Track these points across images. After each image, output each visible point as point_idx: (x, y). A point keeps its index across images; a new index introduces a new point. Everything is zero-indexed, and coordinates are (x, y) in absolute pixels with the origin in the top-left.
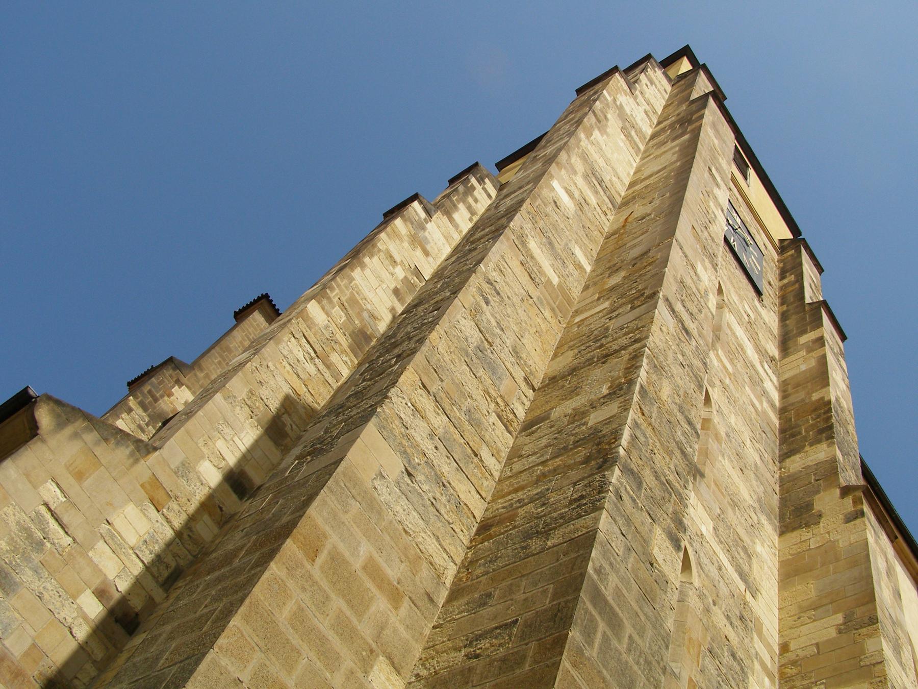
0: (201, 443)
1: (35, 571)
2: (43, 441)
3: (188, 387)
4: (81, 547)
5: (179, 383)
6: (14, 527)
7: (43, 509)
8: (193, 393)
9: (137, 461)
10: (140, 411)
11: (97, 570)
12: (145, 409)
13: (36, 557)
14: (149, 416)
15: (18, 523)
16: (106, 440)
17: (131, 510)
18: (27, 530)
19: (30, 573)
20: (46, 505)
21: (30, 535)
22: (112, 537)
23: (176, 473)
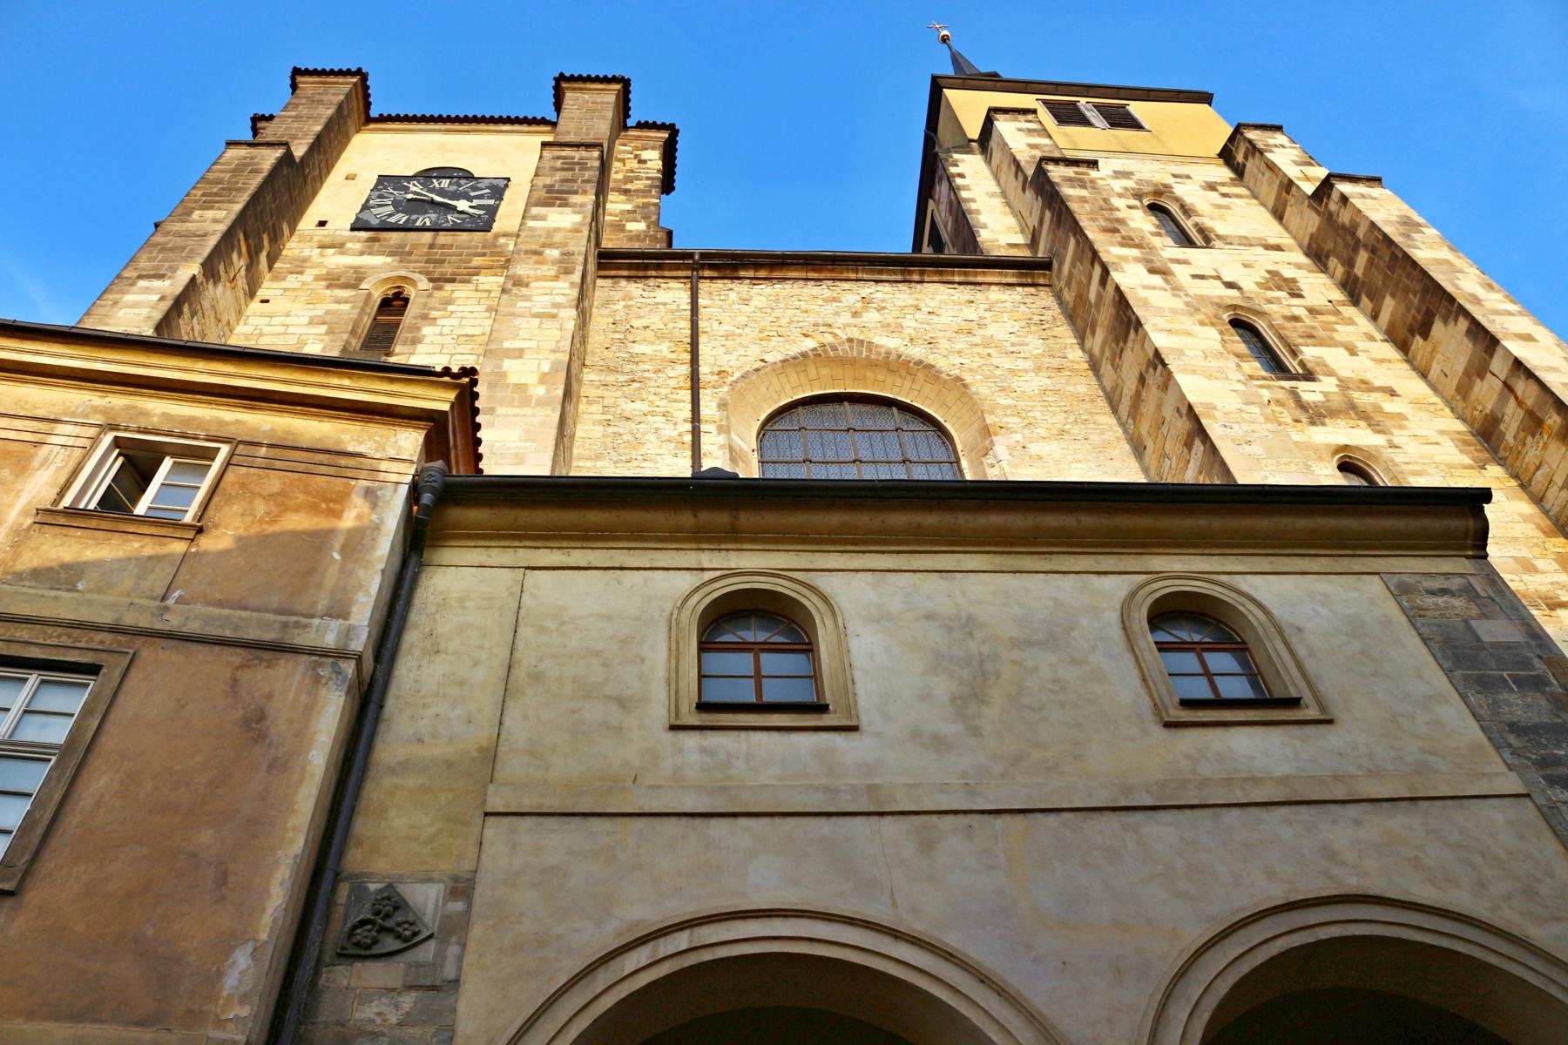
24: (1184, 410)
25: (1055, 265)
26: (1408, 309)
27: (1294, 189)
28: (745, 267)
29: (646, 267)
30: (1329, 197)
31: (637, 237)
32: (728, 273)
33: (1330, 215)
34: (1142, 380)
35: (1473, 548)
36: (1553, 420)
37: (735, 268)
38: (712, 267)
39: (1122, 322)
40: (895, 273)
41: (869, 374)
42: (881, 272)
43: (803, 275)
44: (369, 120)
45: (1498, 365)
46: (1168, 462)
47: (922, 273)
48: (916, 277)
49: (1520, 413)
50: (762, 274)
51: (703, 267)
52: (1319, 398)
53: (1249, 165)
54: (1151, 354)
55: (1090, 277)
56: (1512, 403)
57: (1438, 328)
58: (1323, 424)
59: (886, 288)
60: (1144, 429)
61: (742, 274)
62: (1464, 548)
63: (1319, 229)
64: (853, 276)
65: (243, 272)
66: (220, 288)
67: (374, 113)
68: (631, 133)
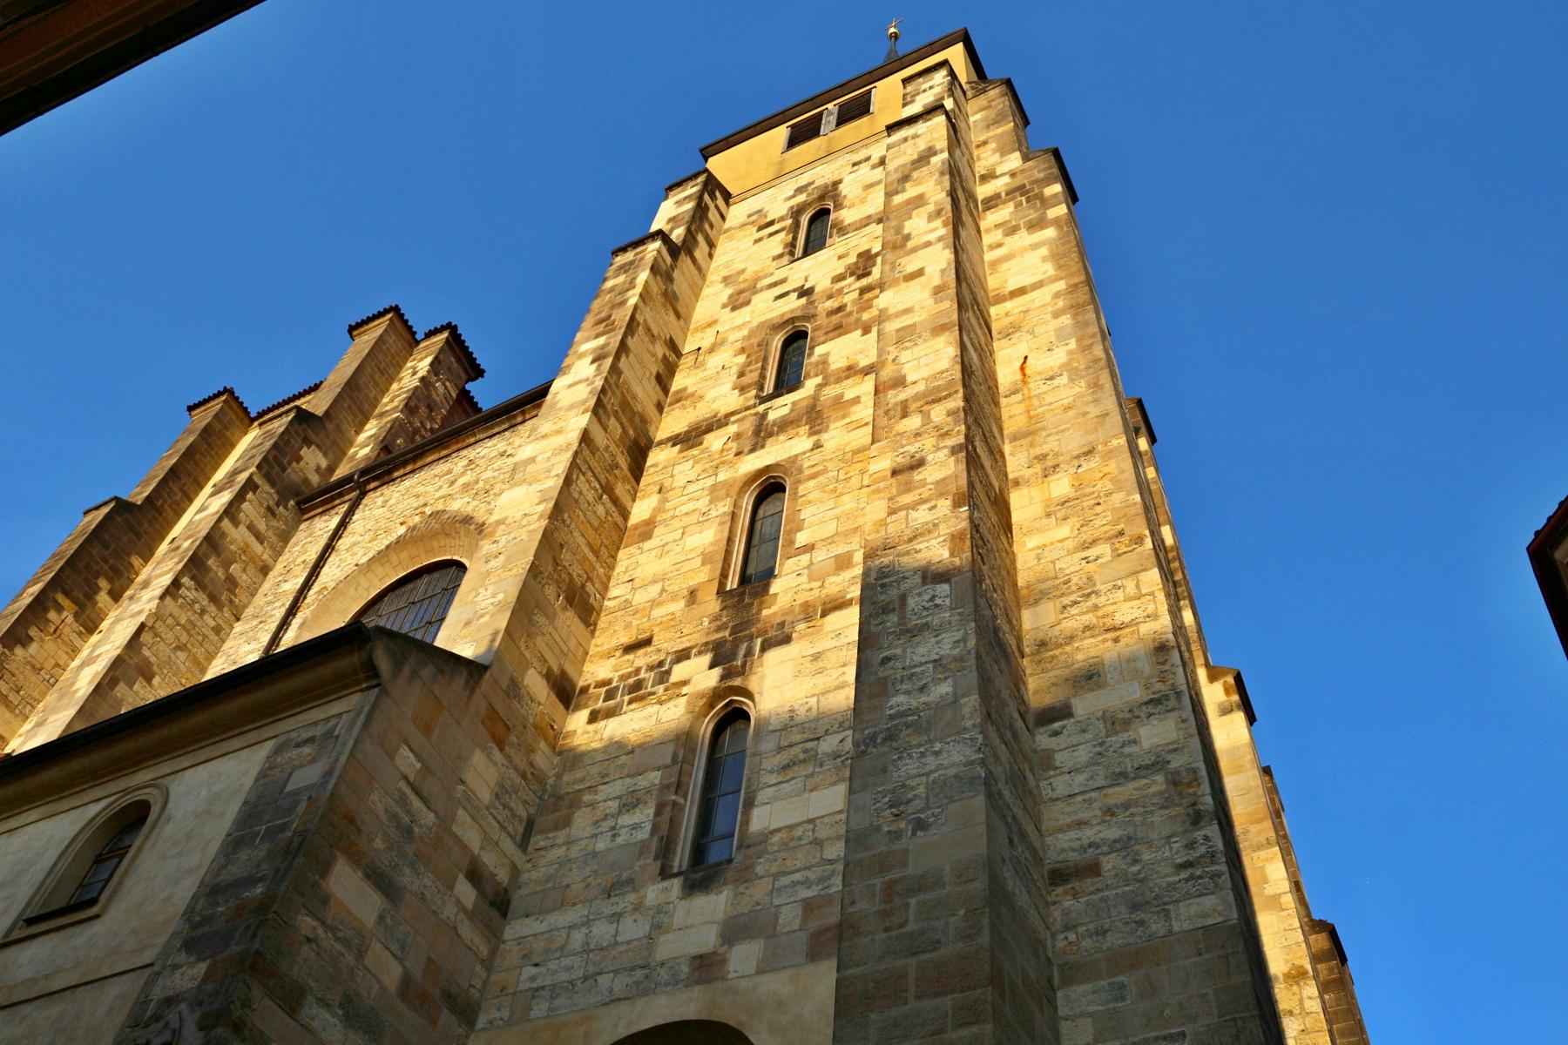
0: (522, 645)
1: (413, 867)
2: (385, 692)
3: (318, 447)
4: (445, 823)
5: (308, 442)
6: (382, 814)
7: (402, 785)
8: (325, 455)
9: (472, 692)
10: (267, 487)
11: (464, 847)
12: (273, 484)
13: (409, 849)
14: (278, 492)
15: (386, 810)
16: (442, 672)
17: (478, 758)
18: (394, 817)
19: (408, 871)
20: (405, 778)
21: (399, 825)
22: (469, 800)
23: (508, 695)
28: (396, 468)
29: (332, 499)
31: (367, 457)
32: (386, 478)
35: (367, 679)
37: (390, 472)
38: (374, 479)
40: (498, 424)
41: (435, 543)
42: (492, 427)
43: (436, 456)
44: (253, 420)
47: (523, 413)
48: (519, 419)
50: (409, 468)
51: (368, 482)
52: (785, 411)
58: (763, 447)
59: (495, 440)
61: (396, 474)
62: (359, 682)
64: (472, 440)
65: (70, 619)
66: (33, 648)
67: (253, 415)
68: (422, 345)
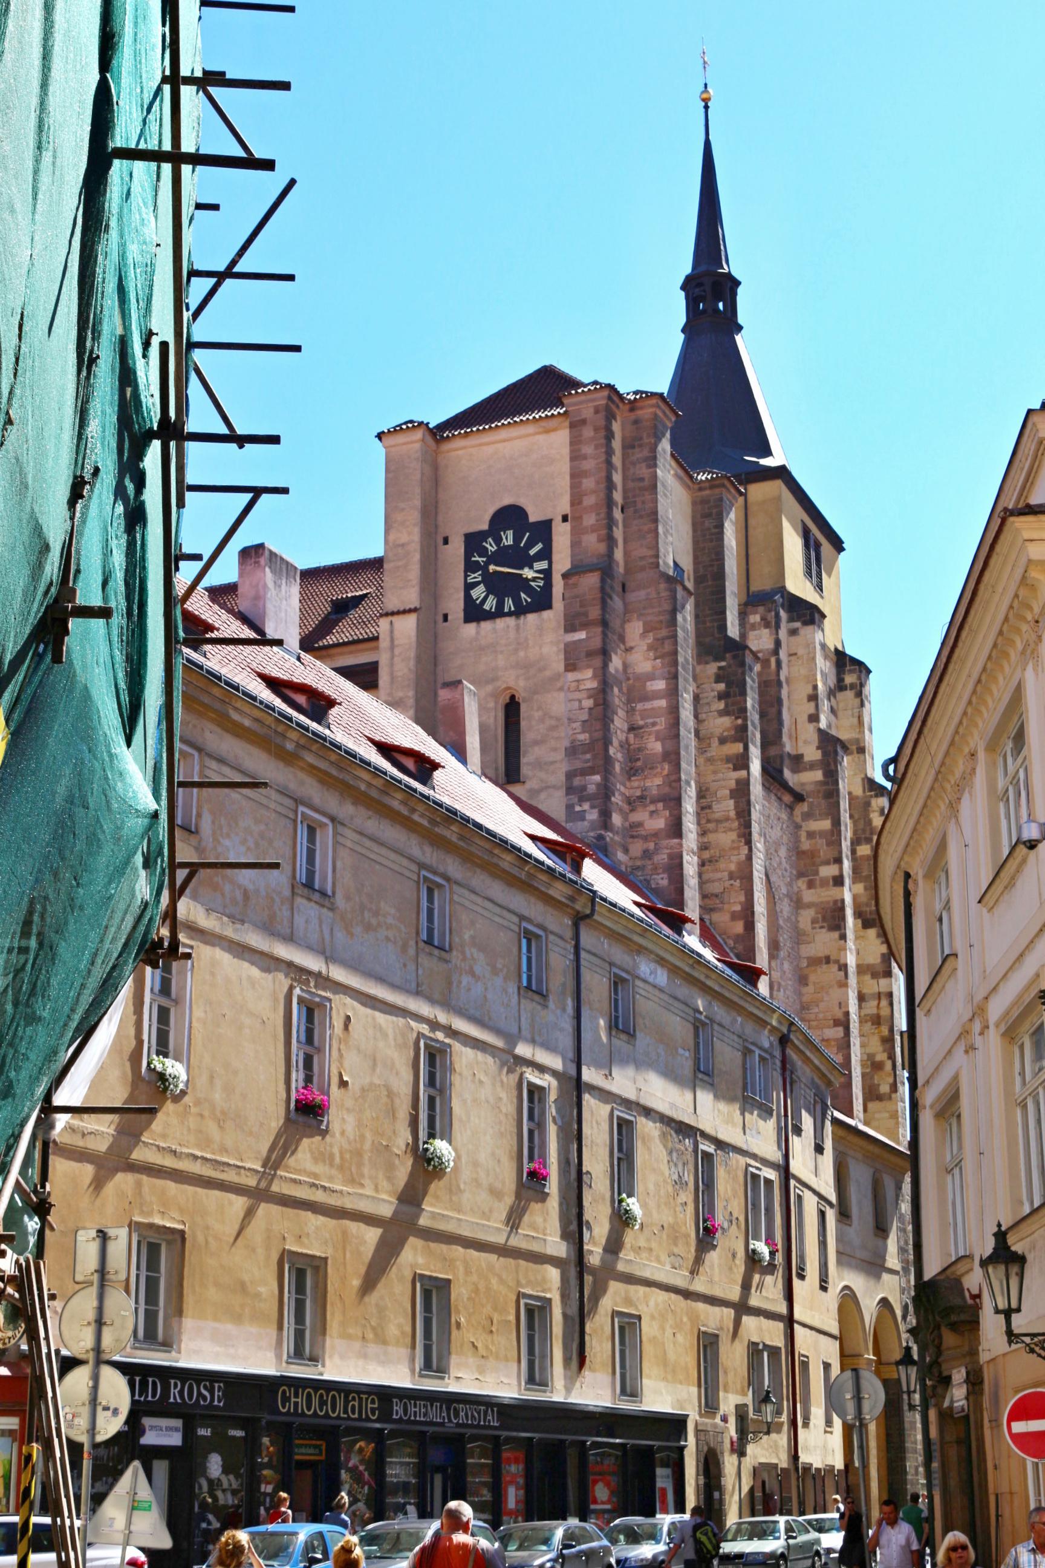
24: (844, 1010)
25: (804, 807)
26: (867, 905)
27: (861, 756)
30: (876, 796)
33: (868, 804)
34: (828, 960)
36: (885, 1031)
39: (833, 917)
45: (883, 982)
46: (816, 1010)
49: (875, 1011)
53: (849, 694)
54: (842, 962)
55: (827, 863)
56: (875, 1003)
57: (872, 932)
60: (812, 978)
63: (857, 797)
